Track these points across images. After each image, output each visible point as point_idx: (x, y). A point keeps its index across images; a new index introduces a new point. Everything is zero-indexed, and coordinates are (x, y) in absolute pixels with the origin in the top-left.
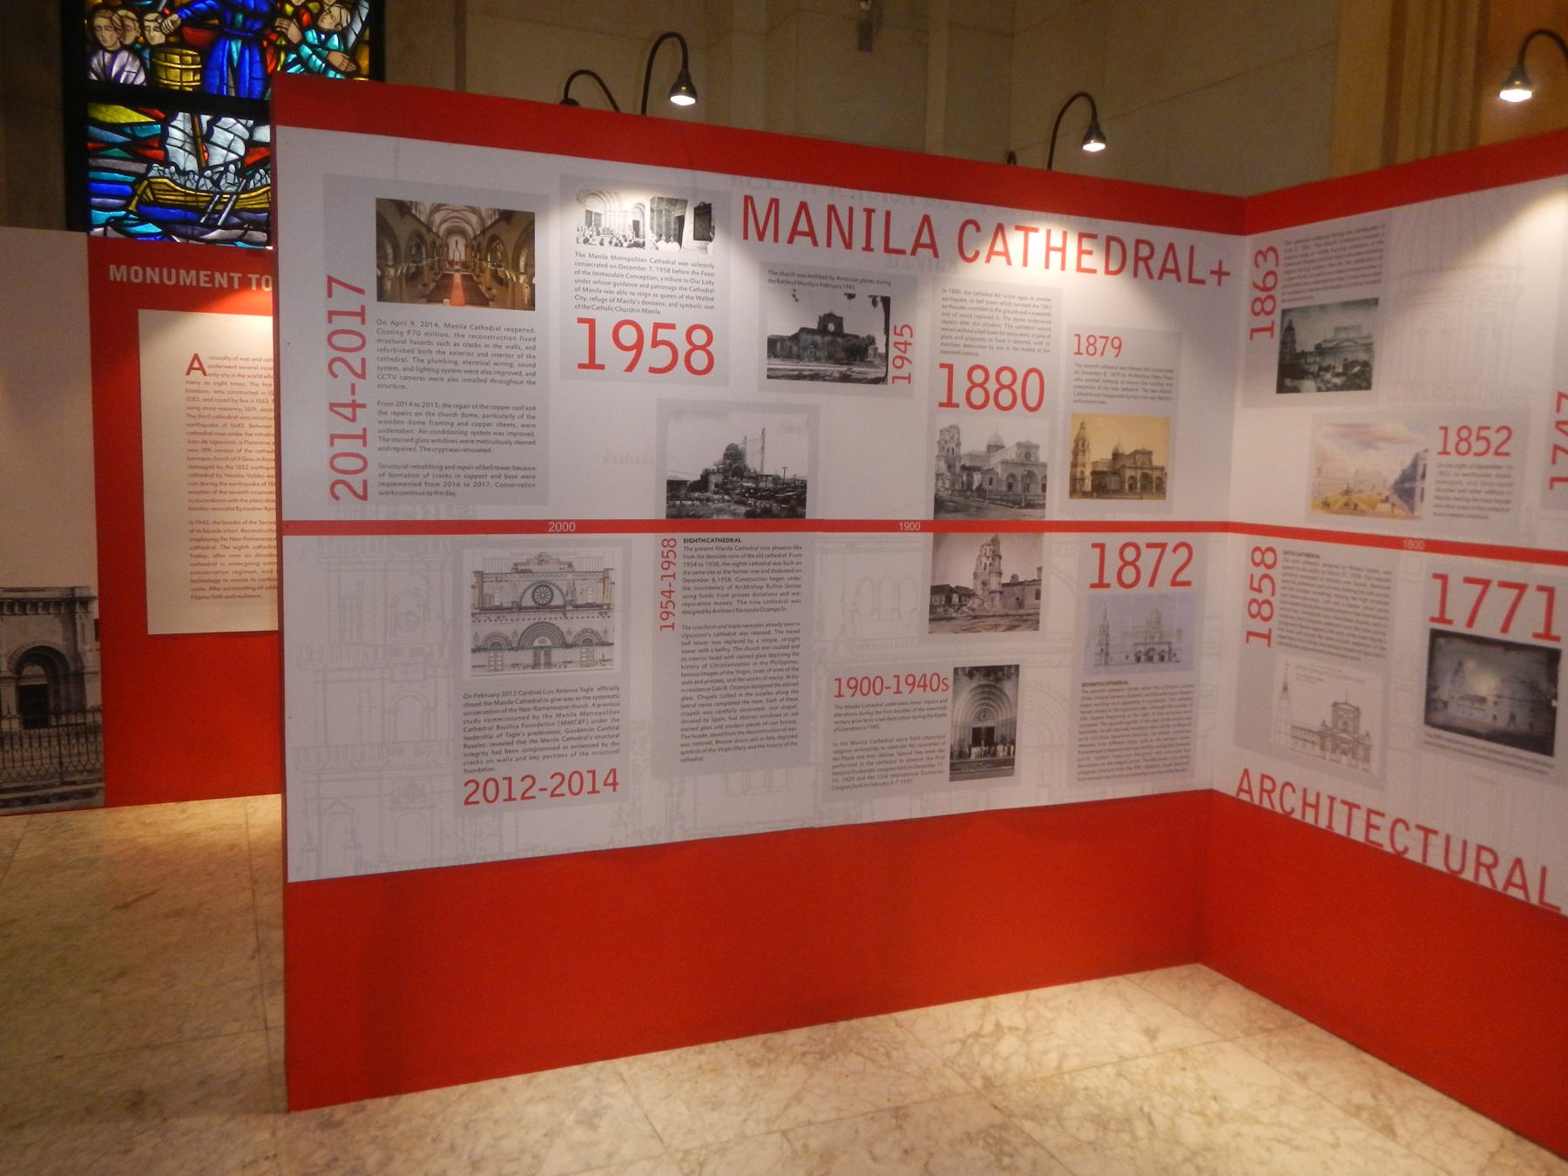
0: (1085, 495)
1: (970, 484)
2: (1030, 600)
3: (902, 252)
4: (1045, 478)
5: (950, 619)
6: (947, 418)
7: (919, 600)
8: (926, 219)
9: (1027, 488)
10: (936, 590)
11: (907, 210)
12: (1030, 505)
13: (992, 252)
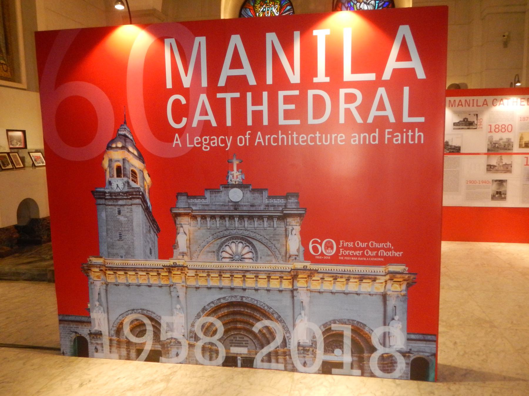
0: (523, 148)
1: (495, 146)
2: (509, 168)
3: (480, 106)
4: (513, 145)
5: (491, 171)
6: (490, 134)
7: (484, 167)
8: (485, 100)
9: (508, 146)
10: (488, 165)
11: (481, 99)
12: (509, 150)
13: (500, 104)
